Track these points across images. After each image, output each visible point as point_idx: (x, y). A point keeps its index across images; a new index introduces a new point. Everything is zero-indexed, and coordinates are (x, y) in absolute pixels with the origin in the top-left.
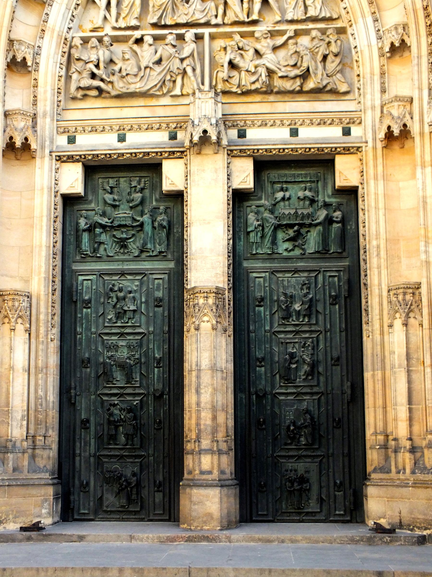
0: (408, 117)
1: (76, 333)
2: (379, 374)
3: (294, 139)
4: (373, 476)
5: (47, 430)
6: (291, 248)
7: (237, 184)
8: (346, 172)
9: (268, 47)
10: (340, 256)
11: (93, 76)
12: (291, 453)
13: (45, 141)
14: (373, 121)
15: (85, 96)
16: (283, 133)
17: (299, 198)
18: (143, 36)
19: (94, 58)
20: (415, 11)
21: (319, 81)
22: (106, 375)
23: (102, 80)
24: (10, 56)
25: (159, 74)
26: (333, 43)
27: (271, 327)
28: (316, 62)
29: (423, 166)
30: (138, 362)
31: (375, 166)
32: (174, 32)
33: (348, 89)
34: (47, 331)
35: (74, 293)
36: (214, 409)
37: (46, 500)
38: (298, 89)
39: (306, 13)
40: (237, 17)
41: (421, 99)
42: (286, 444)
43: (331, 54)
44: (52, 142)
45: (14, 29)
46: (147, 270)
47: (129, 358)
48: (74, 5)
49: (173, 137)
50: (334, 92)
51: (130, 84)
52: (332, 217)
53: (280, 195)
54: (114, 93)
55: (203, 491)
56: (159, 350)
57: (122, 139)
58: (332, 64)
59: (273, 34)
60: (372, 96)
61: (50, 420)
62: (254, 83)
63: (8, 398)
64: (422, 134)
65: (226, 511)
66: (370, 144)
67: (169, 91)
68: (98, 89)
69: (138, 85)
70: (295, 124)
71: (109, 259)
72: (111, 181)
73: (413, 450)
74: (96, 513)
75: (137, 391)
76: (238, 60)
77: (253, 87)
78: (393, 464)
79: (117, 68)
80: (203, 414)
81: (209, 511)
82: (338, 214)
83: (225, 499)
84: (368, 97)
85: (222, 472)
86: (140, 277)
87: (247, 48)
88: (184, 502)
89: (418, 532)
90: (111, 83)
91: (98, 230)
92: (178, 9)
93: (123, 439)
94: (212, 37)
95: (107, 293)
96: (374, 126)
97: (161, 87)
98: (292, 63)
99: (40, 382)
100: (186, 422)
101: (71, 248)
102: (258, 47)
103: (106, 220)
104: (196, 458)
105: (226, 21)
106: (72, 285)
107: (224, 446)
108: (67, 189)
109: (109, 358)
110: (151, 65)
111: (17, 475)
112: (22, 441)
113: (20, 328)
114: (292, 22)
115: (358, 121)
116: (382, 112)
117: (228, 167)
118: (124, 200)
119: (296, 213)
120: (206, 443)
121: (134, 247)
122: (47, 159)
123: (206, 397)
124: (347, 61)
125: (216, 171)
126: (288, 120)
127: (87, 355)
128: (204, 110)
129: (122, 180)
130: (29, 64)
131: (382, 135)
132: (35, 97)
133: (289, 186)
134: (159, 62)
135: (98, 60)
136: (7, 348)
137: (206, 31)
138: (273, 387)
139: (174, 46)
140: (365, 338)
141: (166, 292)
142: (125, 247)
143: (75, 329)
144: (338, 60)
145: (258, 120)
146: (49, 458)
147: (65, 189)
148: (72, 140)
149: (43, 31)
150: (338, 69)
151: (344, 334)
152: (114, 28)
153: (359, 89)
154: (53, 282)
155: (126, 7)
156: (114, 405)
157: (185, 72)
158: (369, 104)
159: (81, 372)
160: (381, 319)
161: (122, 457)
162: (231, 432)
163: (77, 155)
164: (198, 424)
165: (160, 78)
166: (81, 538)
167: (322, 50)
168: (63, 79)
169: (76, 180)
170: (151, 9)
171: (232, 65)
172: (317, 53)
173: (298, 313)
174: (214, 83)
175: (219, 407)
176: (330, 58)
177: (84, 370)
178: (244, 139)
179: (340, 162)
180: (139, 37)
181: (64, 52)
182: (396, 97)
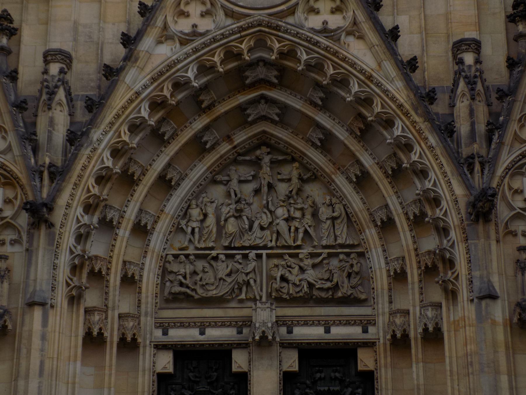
7: (285, 368)
8: (365, 360)
11: (181, 284)
13: (147, 334)
17: (331, 378)
18: (218, 254)
19: (182, 271)
21: (345, 292)
23: (188, 287)
25: (230, 283)
26: (355, 266)
29: (417, 363)
31: (386, 357)
32: (241, 252)
33: (366, 297)
38: (330, 297)
39: (336, 240)
40: (286, 242)
43: (354, 272)
44: (151, 334)
49: (240, 332)
51: (209, 291)
53: (318, 375)
54: (197, 297)
59: (312, 255)
60: (383, 306)
66: (382, 341)
67: (237, 296)
68: (184, 293)
69: (214, 292)
70: (328, 323)
77: (298, 295)
84: (380, 306)
87: (293, 266)
92: (244, 236)
94: (269, 256)
97: (231, 293)
98: (326, 276)
105: (278, 244)
108: (162, 369)
110: (224, 277)
115: (374, 322)
117: (280, 356)
119: (329, 389)
126: (323, 321)
135: (185, 273)
137: (264, 252)
139: (240, 263)
144: (358, 277)
145: (302, 321)
147: (159, 369)
148: (165, 333)
149: (146, 252)
150: (359, 283)
152: (197, 249)
153: (374, 299)
155: (206, 233)
163: (169, 345)
165: (230, 286)
168: (159, 287)
169: (168, 363)
170: (224, 235)
171: (283, 279)
172: (344, 271)
174: (269, 290)
176: (353, 275)
178: (291, 335)
180: (215, 255)
181: (160, 266)
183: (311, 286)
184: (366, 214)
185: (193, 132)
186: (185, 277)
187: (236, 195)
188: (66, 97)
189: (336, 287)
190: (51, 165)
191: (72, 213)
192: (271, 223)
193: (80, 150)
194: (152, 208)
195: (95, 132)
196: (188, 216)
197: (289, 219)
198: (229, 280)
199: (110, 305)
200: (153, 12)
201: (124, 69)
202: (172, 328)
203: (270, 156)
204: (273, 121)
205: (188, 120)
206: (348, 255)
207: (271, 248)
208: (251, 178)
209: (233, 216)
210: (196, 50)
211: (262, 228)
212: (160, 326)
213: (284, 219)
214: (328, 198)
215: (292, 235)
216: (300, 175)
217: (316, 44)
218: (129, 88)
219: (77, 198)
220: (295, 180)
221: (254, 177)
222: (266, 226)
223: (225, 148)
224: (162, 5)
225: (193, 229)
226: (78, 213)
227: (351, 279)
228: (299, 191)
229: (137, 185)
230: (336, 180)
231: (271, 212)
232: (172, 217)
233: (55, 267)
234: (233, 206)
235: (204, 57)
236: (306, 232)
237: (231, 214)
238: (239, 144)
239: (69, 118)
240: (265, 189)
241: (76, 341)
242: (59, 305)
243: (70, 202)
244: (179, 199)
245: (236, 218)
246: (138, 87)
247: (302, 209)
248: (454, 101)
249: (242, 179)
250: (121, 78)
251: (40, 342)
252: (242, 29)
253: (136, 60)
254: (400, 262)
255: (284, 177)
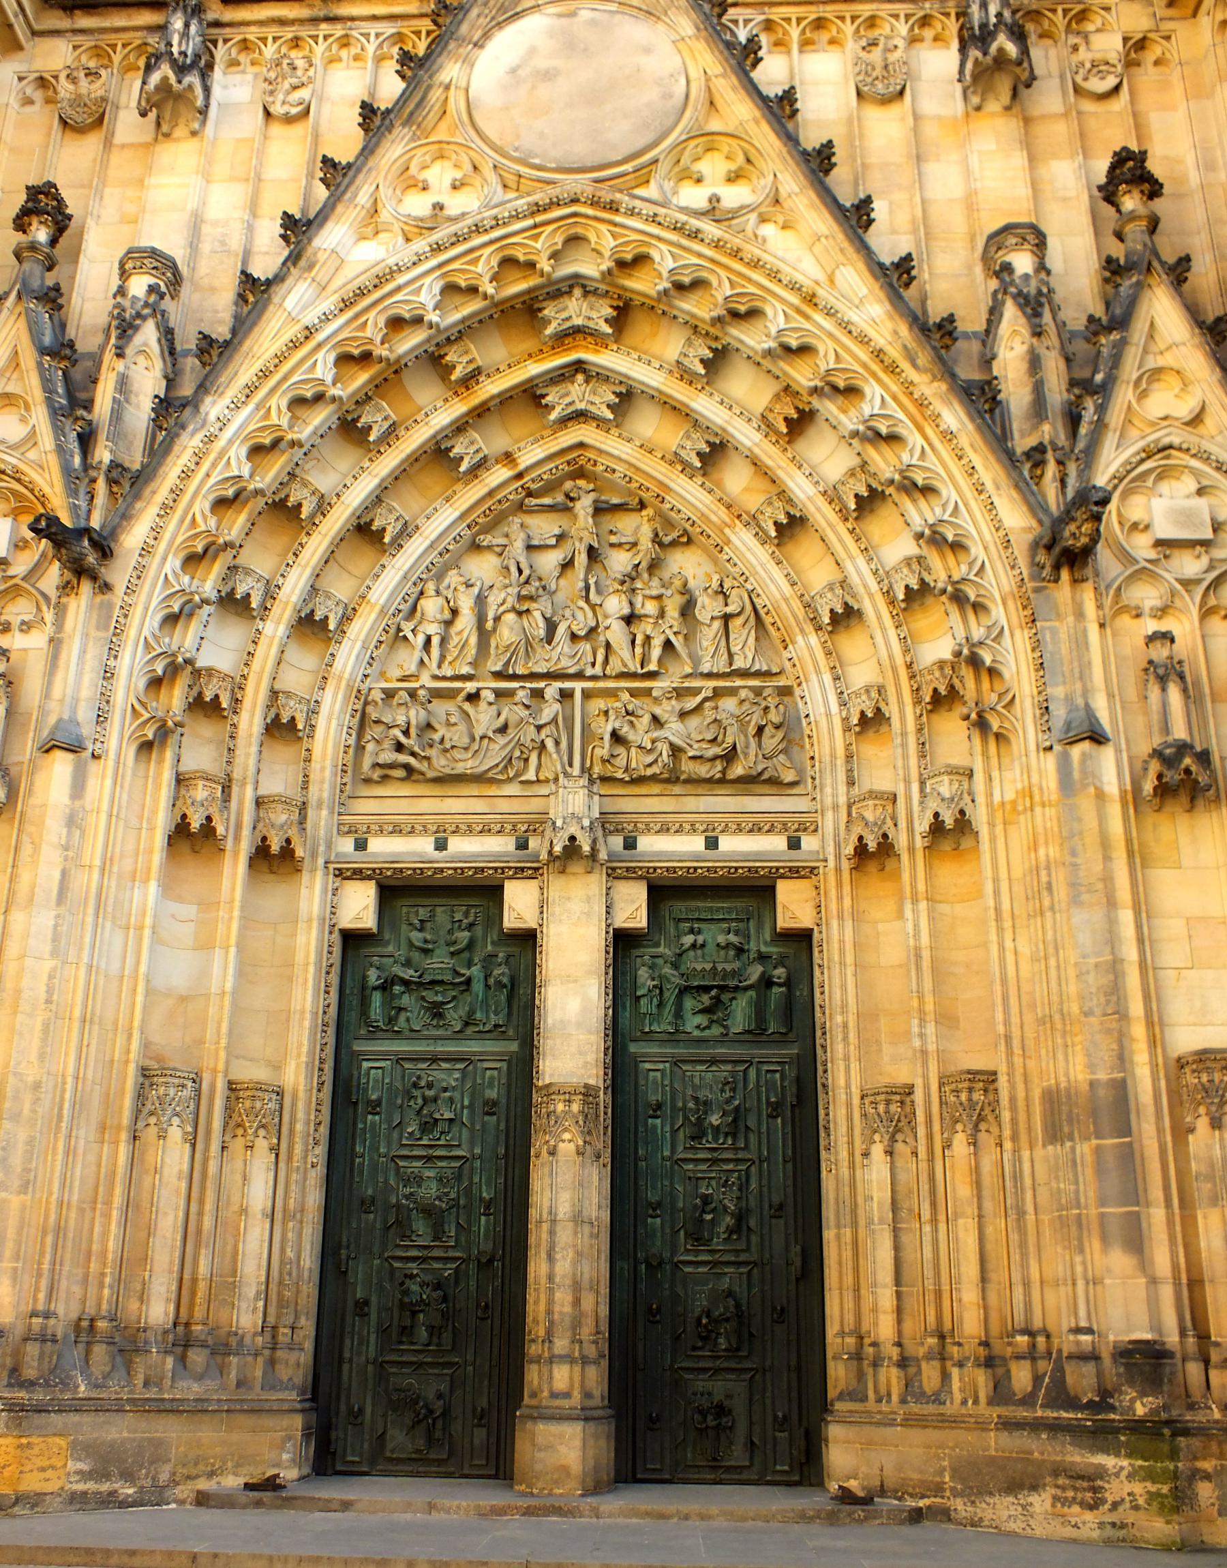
0: (889, 823)
1: (354, 1155)
2: (847, 1233)
3: (711, 854)
4: (838, 1406)
5: (297, 1317)
6: (705, 1023)
7: (621, 921)
8: (793, 906)
9: (672, 711)
10: (782, 1039)
11: (399, 747)
12: (701, 1365)
14: (836, 829)
15: (385, 778)
16: (696, 844)
18: (479, 690)
19: (401, 720)
20: (894, 669)
22: (401, 1226)
23: (413, 754)
24: (272, 715)
26: (773, 709)
27: (673, 1150)
28: (746, 736)
29: (915, 900)
30: (454, 1204)
31: (840, 898)
32: (528, 685)
34: (307, 1151)
35: (354, 1090)
36: (576, 1287)
37: (289, 1438)
38: (718, 776)
40: (625, 666)
41: (909, 798)
42: (694, 1348)
44: (329, 846)
45: (281, 675)
46: (474, 1054)
47: (439, 1198)
48: (374, 643)
49: (522, 845)
50: (775, 782)
52: (771, 977)
53: (688, 940)
55: (554, 1428)
56: (488, 1185)
57: (441, 845)
58: (771, 741)
60: (834, 790)
61: (303, 1301)
62: (650, 765)
63: (235, 1261)
64: (911, 850)
65: (591, 1463)
66: (831, 863)
67: (517, 775)
68: (407, 767)
69: (470, 764)
71: (414, 1035)
72: (421, 911)
73: (903, 1363)
74: (373, 1461)
75: (451, 1254)
76: (625, 730)
77: (649, 772)
78: (870, 1385)
79: (437, 737)
80: (558, 1295)
81: (563, 1462)
82: (780, 971)
83: (591, 1442)
84: (828, 790)
85: (587, 1395)
86: (461, 1066)
87: (640, 712)
88: (522, 1447)
89: (911, 1503)
90: (428, 758)
91: (397, 989)
93: (423, 1333)
94: (587, 695)
95: (408, 1092)
96: (836, 835)
97: (506, 767)
98: (709, 737)
99: (290, 1235)
100: (530, 1308)
101: (353, 1016)
102: (658, 711)
103: (411, 972)
104: (545, 1369)
105: (608, 672)
106: (351, 1075)
107: (591, 1351)
109: (407, 1197)
110: (491, 734)
111: (243, 1394)
112: (255, 1334)
113: (262, 1144)
114: (710, 676)
116: (849, 814)
118: (442, 942)
119: (714, 968)
120: (561, 1344)
121: (454, 1017)
122: (319, 874)
123: (563, 1267)
124: (792, 735)
125: (588, 900)
126: (702, 823)
127: (370, 1192)
128: (572, 805)
129: (439, 910)
130: (300, 727)
131: (849, 850)
132: (306, 776)
133: (703, 926)
134: (503, 729)
136: (239, 1178)
137: (578, 686)
138: (674, 1252)
140: (824, 1174)
141: (503, 1091)
142: (440, 1016)
143: (353, 1149)
146: (298, 1364)
148: (361, 845)
149: (325, 678)
151: (790, 1166)
152: (436, 678)
153: (813, 778)
154: (321, 1069)
156: (412, 1277)
157: (543, 746)
158: (829, 801)
159: (360, 1220)
160: (851, 1143)
161: (420, 1365)
162: (604, 1327)
164: (549, 1312)
166: (346, 1506)
167: (756, 719)
168: (351, 751)
170: (492, 651)
171: (616, 737)
173: (717, 1130)
174: (588, 764)
175: (585, 1284)
176: (768, 730)
177: (364, 1216)
179: (784, 890)
182: (871, 792)
183: (676, 750)
184: (797, 605)
185: (431, 432)
186: (406, 733)
187: (520, 572)
188: (159, 341)
189: (730, 756)
190: (115, 465)
191: (154, 566)
192: (593, 630)
193: (178, 435)
194: (341, 588)
195: (214, 402)
196: (418, 614)
197: (630, 619)
198: (502, 740)
199: (235, 776)
200: (351, 173)
201: (283, 280)
202: (376, 835)
203: (593, 496)
204: (600, 422)
205: (420, 410)
206: (758, 692)
207: (594, 678)
208: (553, 541)
209: (513, 609)
210: (437, 248)
211: (574, 637)
212: (349, 832)
213: (622, 618)
214: (716, 577)
215: (638, 650)
216: (657, 535)
217: (695, 235)
218: (293, 320)
219: (167, 536)
220: (646, 543)
221: (561, 538)
222: (582, 633)
223: (499, 475)
224: (370, 164)
225: (428, 640)
226: (167, 569)
227: (764, 739)
228: (654, 566)
229: (308, 534)
230: (733, 538)
231: (593, 607)
232: (382, 612)
233: (108, 674)
234: (514, 591)
235: (456, 265)
236: (668, 645)
237: (508, 605)
238: (528, 469)
239: (164, 383)
240: (581, 559)
241: (151, 839)
242: (112, 755)
243: (152, 542)
244: (401, 573)
245: (520, 614)
246: (311, 318)
247: (659, 597)
248: (992, 348)
249: (535, 542)
250: (276, 300)
251: (65, 831)
252: (538, 209)
253: (311, 267)
254: (874, 694)
255: (623, 540)
